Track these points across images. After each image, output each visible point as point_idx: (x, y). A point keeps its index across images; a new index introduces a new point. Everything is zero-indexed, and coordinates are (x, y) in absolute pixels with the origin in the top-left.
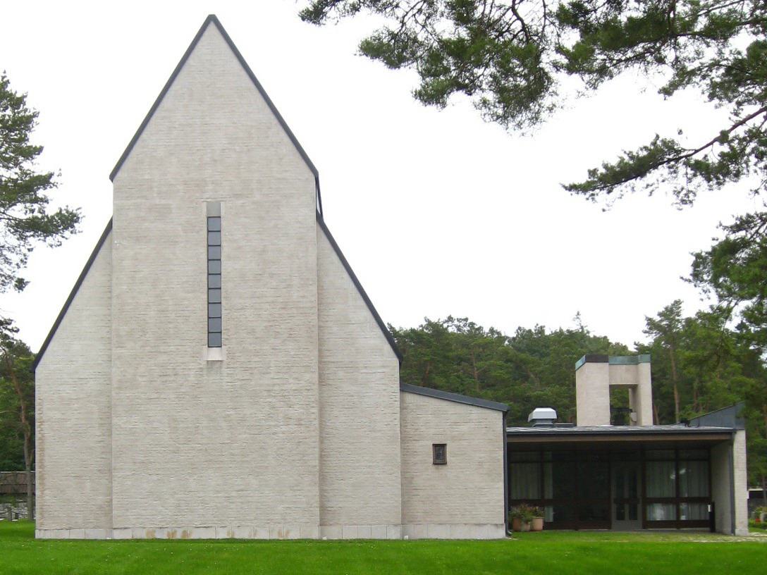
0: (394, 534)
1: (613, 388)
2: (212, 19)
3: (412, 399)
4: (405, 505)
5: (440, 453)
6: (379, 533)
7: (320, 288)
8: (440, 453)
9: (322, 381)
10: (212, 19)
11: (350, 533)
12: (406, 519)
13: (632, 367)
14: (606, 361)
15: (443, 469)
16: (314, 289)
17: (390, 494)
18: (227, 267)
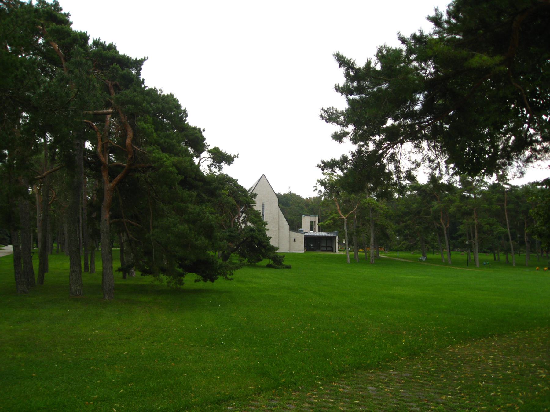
0: (288, 252)
1: (311, 222)
2: (263, 174)
3: (291, 232)
4: (290, 247)
5: (295, 240)
6: (286, 252)
7: (279, 215)
8: (295, 240)
9: (279, 229)
10: (263, 174)
11: (282, 252)
12: (290, 249)
13: (314, 217)
14: (309, 216)
15: (295, 242)
16: (278, 216)
17: (287, 246)
18: (265, 212)
